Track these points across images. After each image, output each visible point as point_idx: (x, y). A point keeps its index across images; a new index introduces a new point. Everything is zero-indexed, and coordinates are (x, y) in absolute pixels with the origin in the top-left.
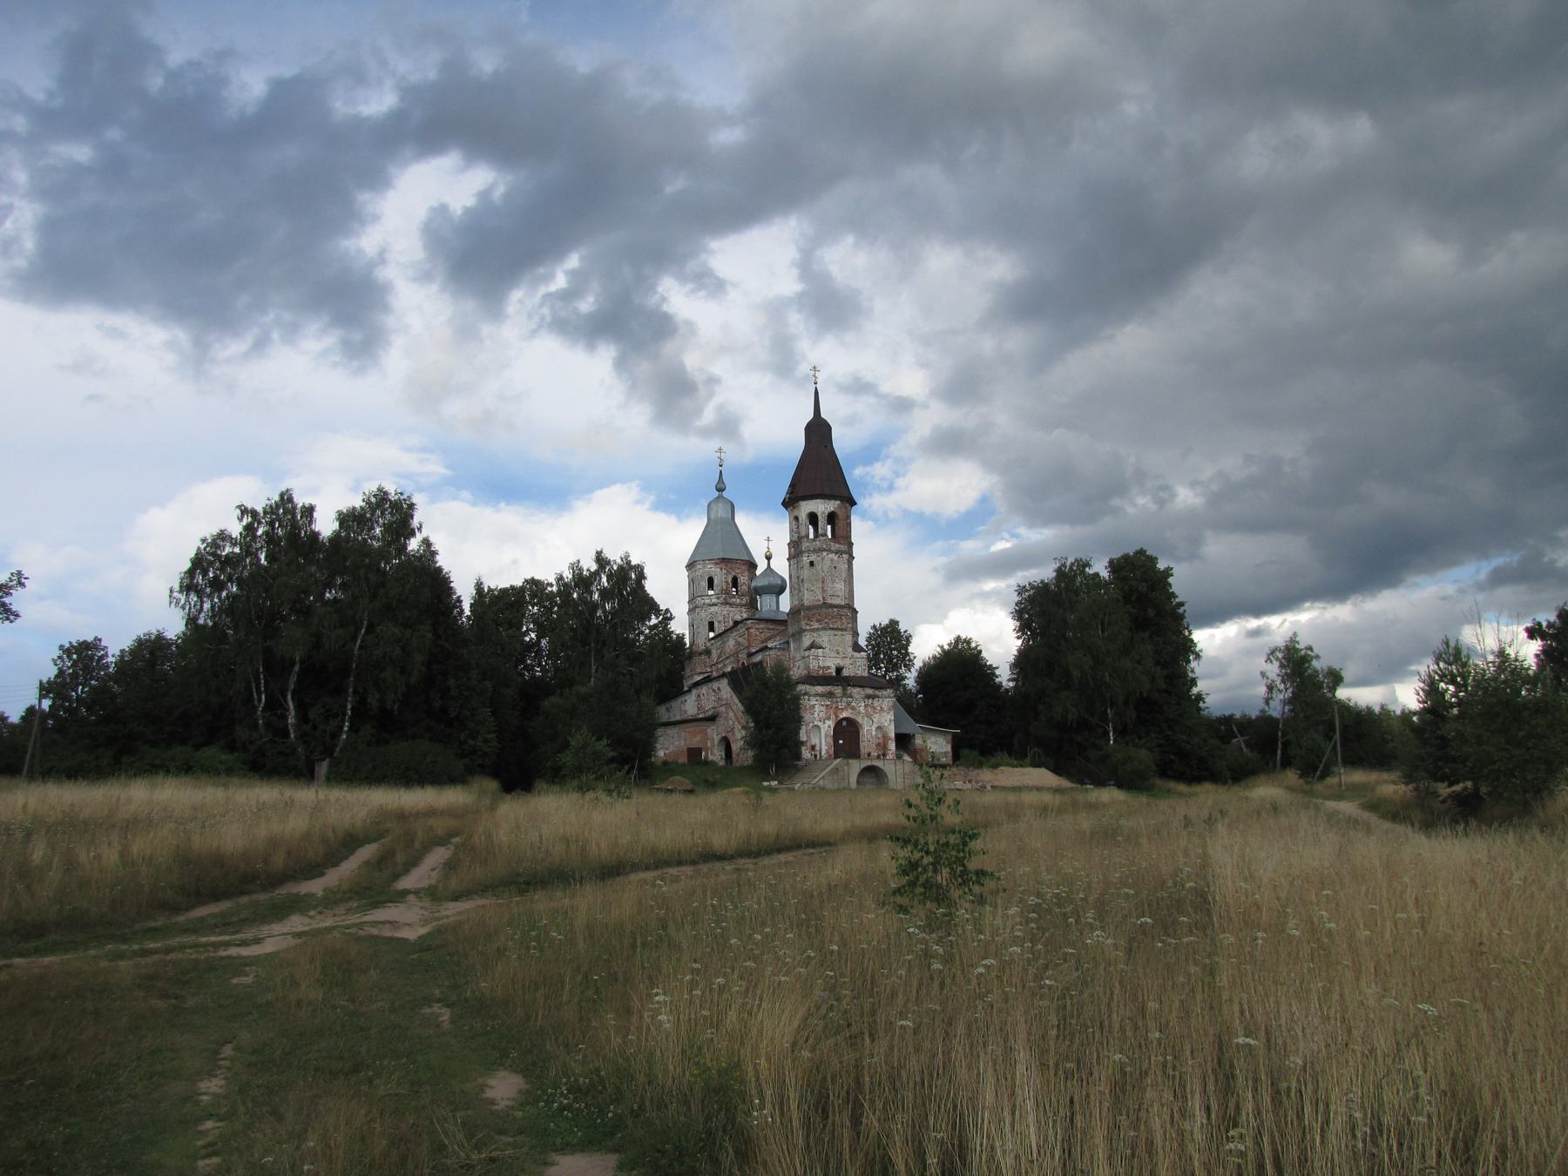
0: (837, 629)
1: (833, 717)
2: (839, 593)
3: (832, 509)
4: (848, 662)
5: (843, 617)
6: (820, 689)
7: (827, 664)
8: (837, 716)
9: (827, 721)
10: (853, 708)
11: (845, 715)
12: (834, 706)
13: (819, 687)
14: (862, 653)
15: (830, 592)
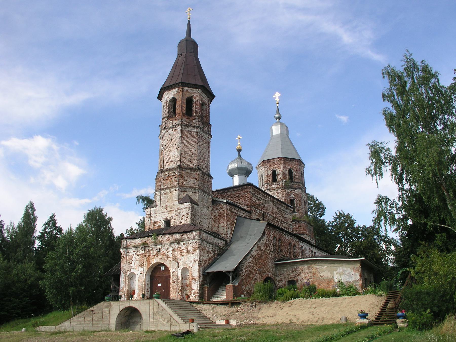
1: (146, 263)
2: (173, 159)
3: (173, 96)
4: (174, 213)
5: (172, 178)
6: (137, 241)
7: (156, 220)
8: (149, 263)
10: (163, 254)
11: (155, 261)
12: (147, 255)
15: (166, 160)
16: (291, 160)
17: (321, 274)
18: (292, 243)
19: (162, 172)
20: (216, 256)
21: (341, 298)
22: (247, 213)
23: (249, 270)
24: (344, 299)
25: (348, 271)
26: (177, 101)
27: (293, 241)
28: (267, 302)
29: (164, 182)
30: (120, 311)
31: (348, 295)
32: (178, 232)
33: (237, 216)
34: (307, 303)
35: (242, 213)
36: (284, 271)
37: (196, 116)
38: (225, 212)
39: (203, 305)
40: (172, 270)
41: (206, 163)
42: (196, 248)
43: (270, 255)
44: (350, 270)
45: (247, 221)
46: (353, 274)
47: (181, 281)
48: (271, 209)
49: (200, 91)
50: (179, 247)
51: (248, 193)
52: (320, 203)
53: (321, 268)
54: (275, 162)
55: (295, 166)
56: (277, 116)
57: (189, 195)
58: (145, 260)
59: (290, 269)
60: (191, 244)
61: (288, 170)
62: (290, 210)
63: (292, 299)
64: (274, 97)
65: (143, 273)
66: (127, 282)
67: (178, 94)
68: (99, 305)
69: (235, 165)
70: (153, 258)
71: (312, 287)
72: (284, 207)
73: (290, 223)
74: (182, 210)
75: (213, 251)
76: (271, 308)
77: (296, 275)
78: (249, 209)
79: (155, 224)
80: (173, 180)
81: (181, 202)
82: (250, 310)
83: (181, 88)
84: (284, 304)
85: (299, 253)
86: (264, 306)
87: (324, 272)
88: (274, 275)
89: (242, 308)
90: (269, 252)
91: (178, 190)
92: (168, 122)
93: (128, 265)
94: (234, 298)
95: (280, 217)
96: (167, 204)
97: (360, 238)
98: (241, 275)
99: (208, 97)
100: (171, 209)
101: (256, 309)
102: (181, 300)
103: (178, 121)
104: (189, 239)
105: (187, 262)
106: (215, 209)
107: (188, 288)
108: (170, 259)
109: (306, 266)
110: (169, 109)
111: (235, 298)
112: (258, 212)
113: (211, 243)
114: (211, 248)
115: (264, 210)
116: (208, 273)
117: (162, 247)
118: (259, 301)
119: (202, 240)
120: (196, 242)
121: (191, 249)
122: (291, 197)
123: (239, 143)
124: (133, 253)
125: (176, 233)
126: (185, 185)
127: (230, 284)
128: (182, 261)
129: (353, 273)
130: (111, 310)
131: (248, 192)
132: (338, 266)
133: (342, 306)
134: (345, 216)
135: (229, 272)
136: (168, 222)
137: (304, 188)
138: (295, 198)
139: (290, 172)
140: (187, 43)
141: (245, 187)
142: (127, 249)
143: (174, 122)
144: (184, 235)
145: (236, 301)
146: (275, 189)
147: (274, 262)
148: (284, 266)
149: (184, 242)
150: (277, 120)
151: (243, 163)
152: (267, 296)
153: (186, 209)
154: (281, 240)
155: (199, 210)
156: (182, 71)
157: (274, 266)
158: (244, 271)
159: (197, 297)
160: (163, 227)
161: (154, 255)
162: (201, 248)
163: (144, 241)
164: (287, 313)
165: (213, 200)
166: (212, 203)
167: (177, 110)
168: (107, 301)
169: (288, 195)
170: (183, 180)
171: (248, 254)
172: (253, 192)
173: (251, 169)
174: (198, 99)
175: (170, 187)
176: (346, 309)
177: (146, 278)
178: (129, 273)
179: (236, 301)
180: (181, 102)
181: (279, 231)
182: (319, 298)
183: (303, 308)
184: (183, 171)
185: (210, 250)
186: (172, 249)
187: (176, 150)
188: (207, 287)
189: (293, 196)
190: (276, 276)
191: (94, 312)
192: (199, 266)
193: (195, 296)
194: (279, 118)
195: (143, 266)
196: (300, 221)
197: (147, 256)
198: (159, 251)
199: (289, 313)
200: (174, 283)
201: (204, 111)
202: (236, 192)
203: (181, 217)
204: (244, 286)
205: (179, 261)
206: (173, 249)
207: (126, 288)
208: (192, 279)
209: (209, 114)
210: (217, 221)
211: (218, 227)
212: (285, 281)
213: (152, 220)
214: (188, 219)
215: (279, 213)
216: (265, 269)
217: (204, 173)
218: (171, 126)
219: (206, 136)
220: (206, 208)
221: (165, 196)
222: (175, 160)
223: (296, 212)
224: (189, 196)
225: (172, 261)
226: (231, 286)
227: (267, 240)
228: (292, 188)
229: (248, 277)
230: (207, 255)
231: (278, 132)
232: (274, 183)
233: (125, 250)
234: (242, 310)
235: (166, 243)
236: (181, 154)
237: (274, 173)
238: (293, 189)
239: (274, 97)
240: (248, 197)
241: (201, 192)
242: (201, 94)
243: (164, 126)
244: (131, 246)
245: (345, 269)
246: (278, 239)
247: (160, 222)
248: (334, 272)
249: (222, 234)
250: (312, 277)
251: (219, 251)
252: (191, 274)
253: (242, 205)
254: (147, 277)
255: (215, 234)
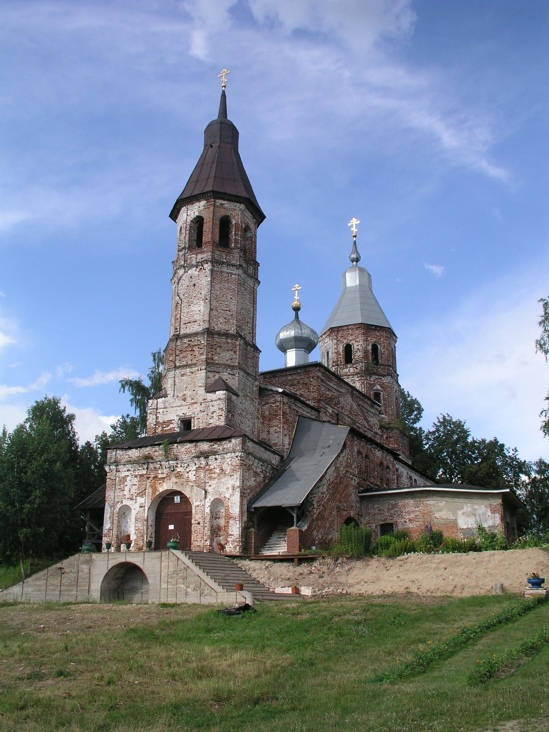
0: (187, 366)
1: (149, 491)
2: (197, 317)
3: (197, 214)
4: (198, 408)
7: (167, 418)
8: (155, 489)
9: (138, 498)
12: (153, 476)
13: (134, 450)
14: (217, 392)
15: (185, 319)
16: (376, 329)
17: (437, 515)
18: (385, 463)
19: (177, 339)
20: (267, 481)
21: (485, 554)
22: (313, 411)
23: (323, 506)
24: (491, 554)
25: (480, 511)
26: (205, 221)
27: (386, 460)
28: (361, 559)
29: (181, 356)
30: (109, 569)
31: (494, 549)
32: (206, 438)
33: (299, 416)
34: (431, 560)
35: (306, 412)
36: (375, 508)
37: (236, 247)
38: (280, 408)
39: (249, 562)
40: (195, 503)
41: (249, 326)
42: (237, 467)
43: (353, 481)
44: (485, 509)
45: (315, 425)
46: (489, 516)
47: (211, 521)
48: (349, 406)
49: (242, 206)
50: (207, 464)
51: (315, 379)
52: (415, 402)
53: (436, 505)
54: (351, 332)
55: (382, 339)
56: (354, 256)
57: (223, 378)
58: (148, 485)
59: (385, 505)
60: (229, 460)
61: (371, 345)
62: (377, 409)
63: (405, 554)
64: (349, 225)
65: (144, 507)
66: (115, 521)
67: (207, 210)
68: (72, 558)
69: (290, 333)
70: (162, 481)
71: (437, 534)
72: (368, 404)
73: (376, 430)
74: (212, 403)
75: (262, 472)
76: (369, 567)
77: (395, 516)
78: (316, 405)
79: (165, 426)
80: (196, 353)
81: (210, 389)
82: (333, 570)
83: (212, 200)
84: (392, 561)
85: (394, 480)
86: (357, 564)
87: (441, 510)
88: (358, 515)
89: (319, 567)
90: (351, 476)
91: (205, 369)
92: (189, 257)
93: (118, 493)
94: (300, 550)
95: (362, 420)
96: (185, 392)
97: (476, 459)
98: (310, 512)
99: (254, 217)
100: (193, 401)
101: (344, 569)
102: (209, 552)
103: (205, 255)
104: (226, 451)
105: (220, 490)
106: (263, 403)
107: (222, 533)
108: (192, 484)
109: (411, 501)
110: (190, 234)
111: (303, 550)
112: (330, 410)
113: (260, 459)
114: (260, 467)
115: (339, 408)
116: (255, 508)
117: (177, 464)
118: (348, 556)
119: (247, 454)
120: (237, 457)
121: (227, 468)
122: (375, 388)
123: (296, 297)
124: (127, 473)
125: (203, 440)
126: (217, 362)
127: (294, 528)
128: (212, 487)
129: (489, 513)
130: (92, 568)
131: (315, 378)
132: (465, 502)
133: (490, 566)
134: (453, 424)
135: (292, 508)
136: (186, 423)
137: (396, 375)
138: (382, 391)
139: (375, 348)
140: (221, 127)
141: (311, 369)
142: (117, 466)
143: (199, 256)
144: (216, 443)
145: (308, 555)
146: (349, 375)
147: (359, 492)
148: (376, 500)
149: (217, 456)
150: (353, 262)
151: (303, 331)
152: (362, 548)
153: (219, 402)
154: (369, 458)
155: (239, 403)
156: (213, 173)
157: (358, 499)
158: (316, 506)
159: (238, 548)
160: (178, 431)
161: (163, 477)
162: (245, 466)
163: (147, 453)
164: (398, 577)
165: (260, 388)
166: (259, 393)
167: (204, 237)
168: (86, 553)
169: (371, 386)
170: (213, 353)
171: (321, 480)
172: (323, 378)
173: (316, 341)
174: (239, 220)
175: (191, 365)
176: (497, 572)
177: (149, 515)
178: (119, 506)
179: (308, 555)
180: (211, 223)
181: (366, 443)
182: (448, 552)
183: (425, 569)
184: (213, 338)
185: (259, 470)
186: (194, 468)
187: (202, 303)
188: (255, 532)
189: (379, 388)
190: (361, 516)
191: (63, 571)
192: (242, 496)
193: (234, 547)
194: (357, 260)
195: (144, 495)
196: (390, 428)
197: (151, 479)
198: (172, 471)
199: (402, 577)
200: (199, 523)
201: (247, 240)
202: (294, 377)
203: (210, 414)
204: (315, 532)
205: (207, 488)
206: (197, 468)
207: (115, 532)
208: (229, 517)
209: (255, 246)
210: (266, 422)
211: (269, 434)
212: (377, 524)
213: (160, 418)
214: (223, 419)
215: (359, 413)
216: (345, 505)
217: (246, 343)
218: (194, 263)
219: (250, 282)
220: (249, 401)
221: (182, 379)
222: (199, 320)
223: (383, 414)
224: (223, 380)
225: (195, 488)
226: (295, 530)
227: (349, 456)
228: (377, 375)
229: (321, 517)
230: (254, 479)
231: (355, 282)
232: (349, 366)
233: (113, 467)
234: (319, 570)
235: (185, 457)
236: (211, 310)
237: (348, 349)
238: (379, 375)
239: (349, 225)
240: (315, 386)
241: (242, 373)
242: (245, 213)
243: (182, 263)
244: (123, 461)
245: (477, 507)
246: (364, 456)
247: (173, 422)
248: (458, 511)
249: (276, 445)
250: (422, 520)
251: (271, 472)
252: (227, 510)
253: (304, 398)
254: (151, 513)
255: (264, 444)
